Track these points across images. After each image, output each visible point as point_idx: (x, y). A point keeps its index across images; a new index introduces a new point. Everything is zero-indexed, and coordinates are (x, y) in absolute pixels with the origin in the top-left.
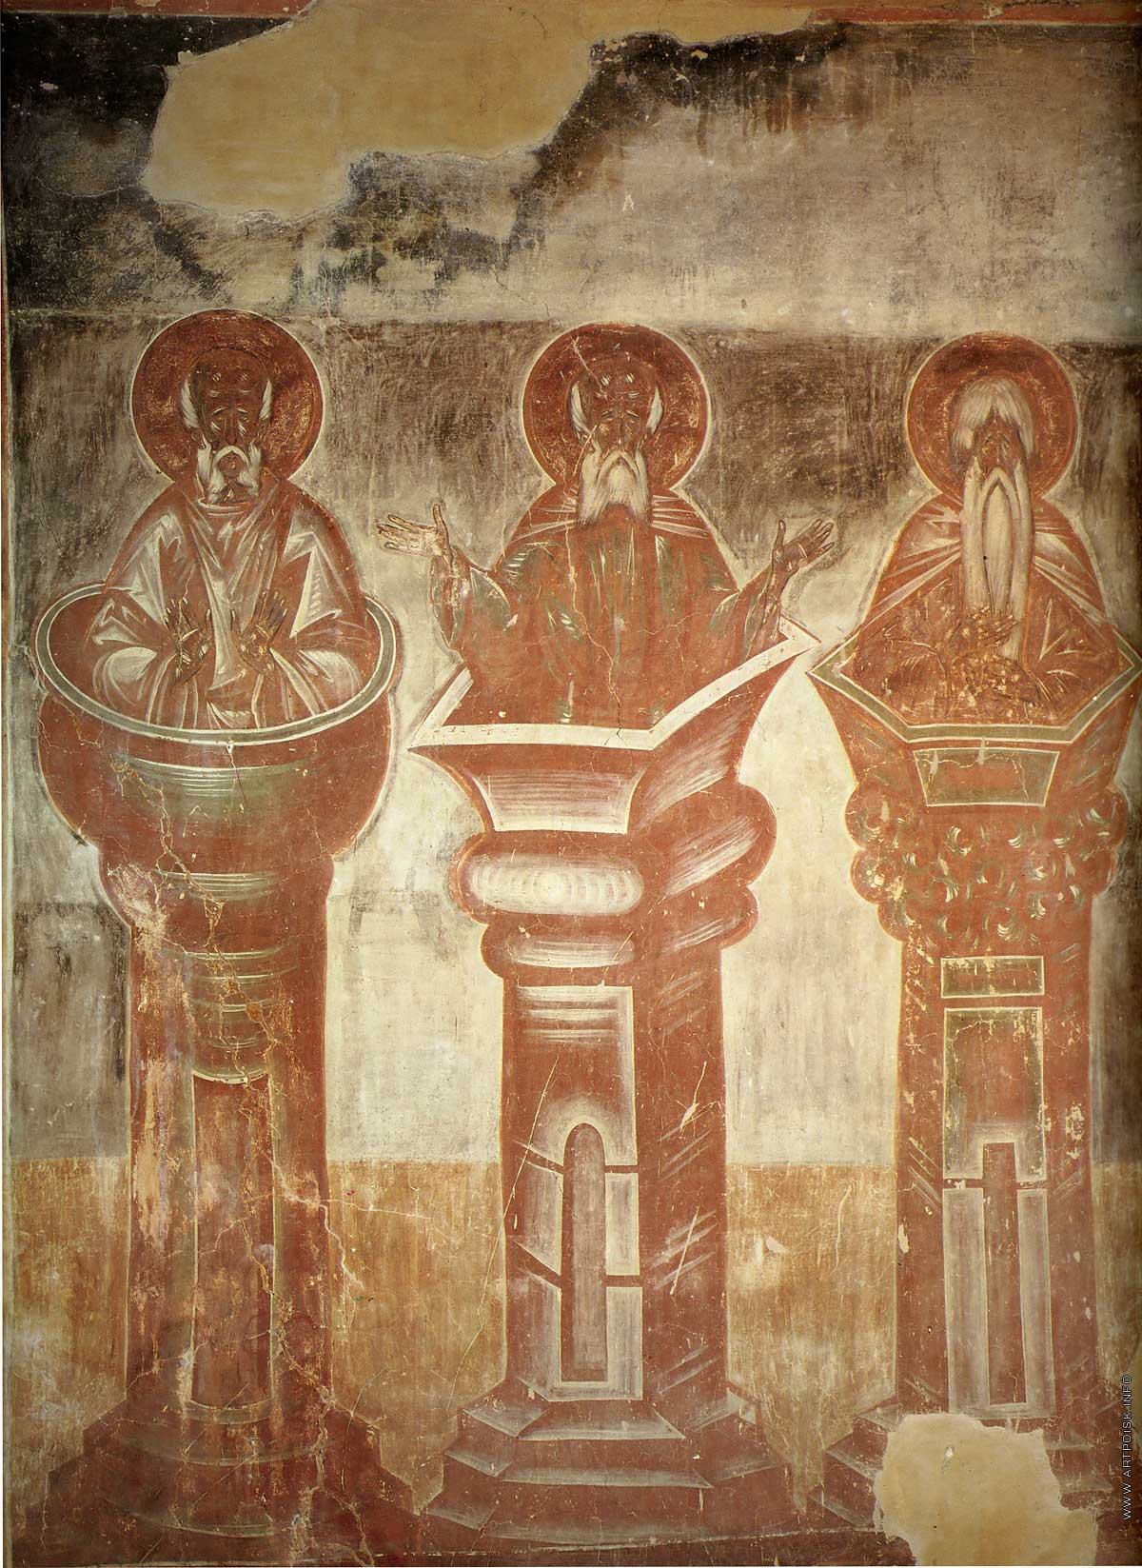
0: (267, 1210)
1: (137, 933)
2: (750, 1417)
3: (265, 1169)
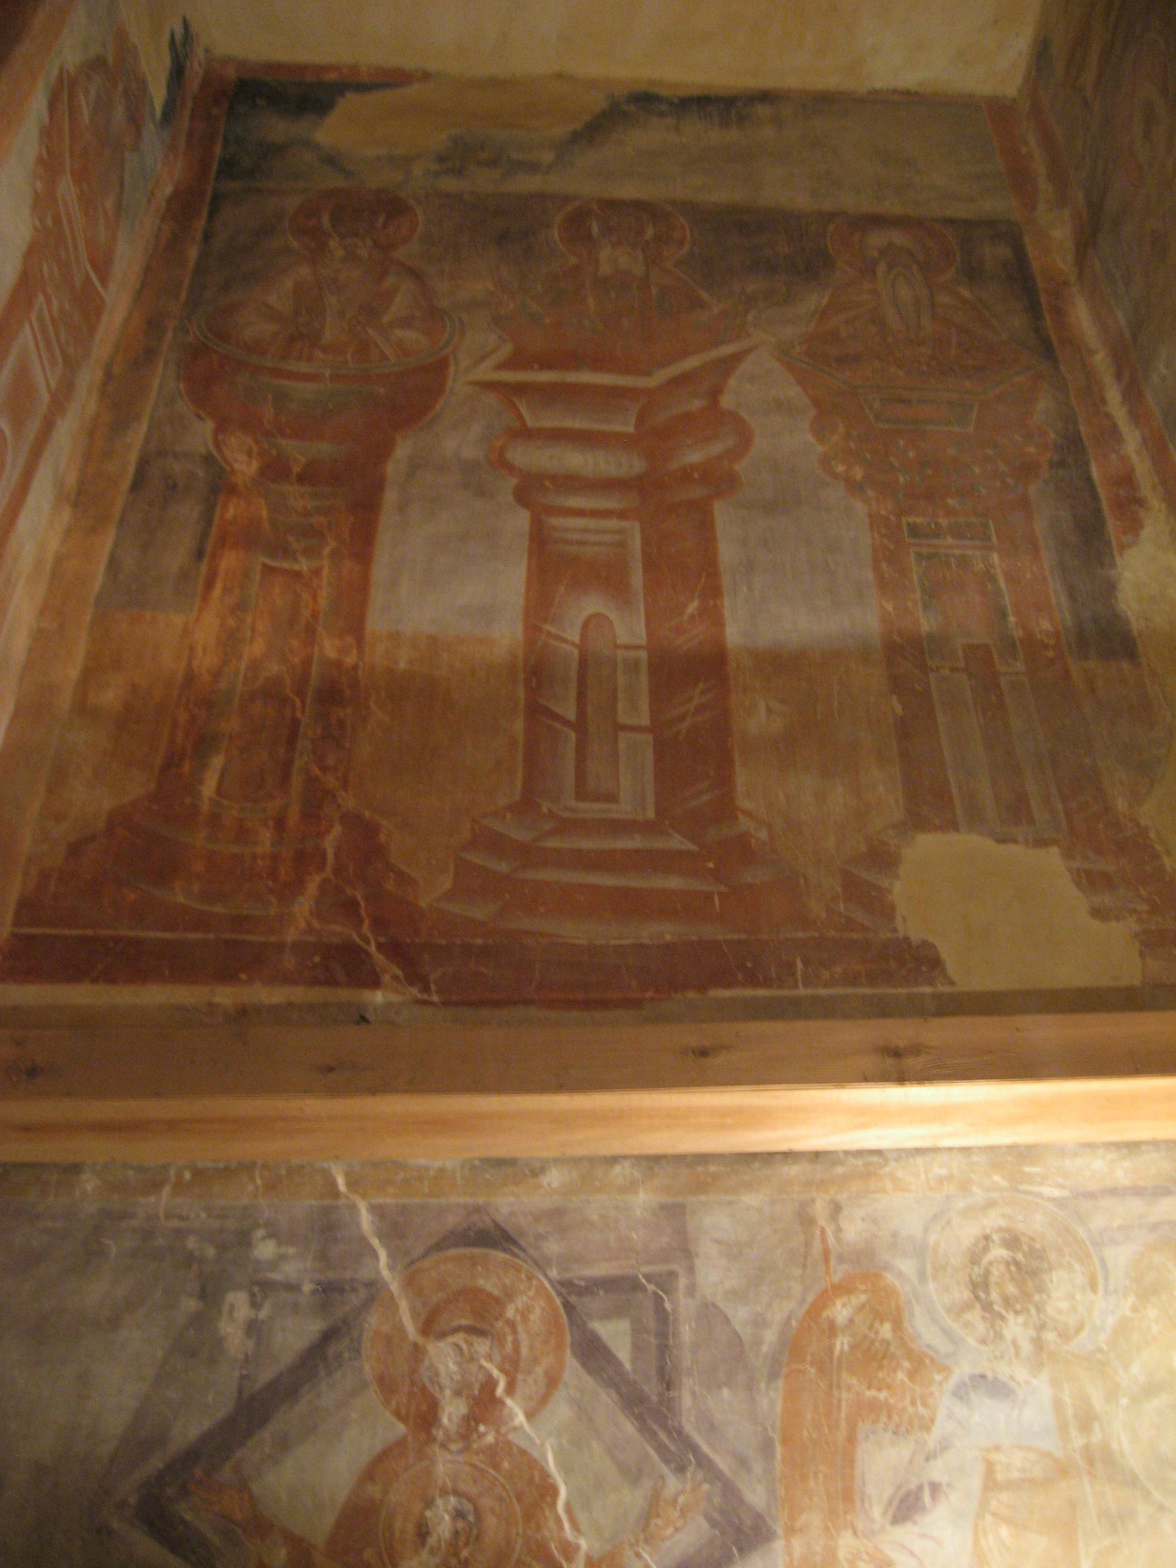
1: (233, 472)
2: (763, 835)
3: (310, 633)
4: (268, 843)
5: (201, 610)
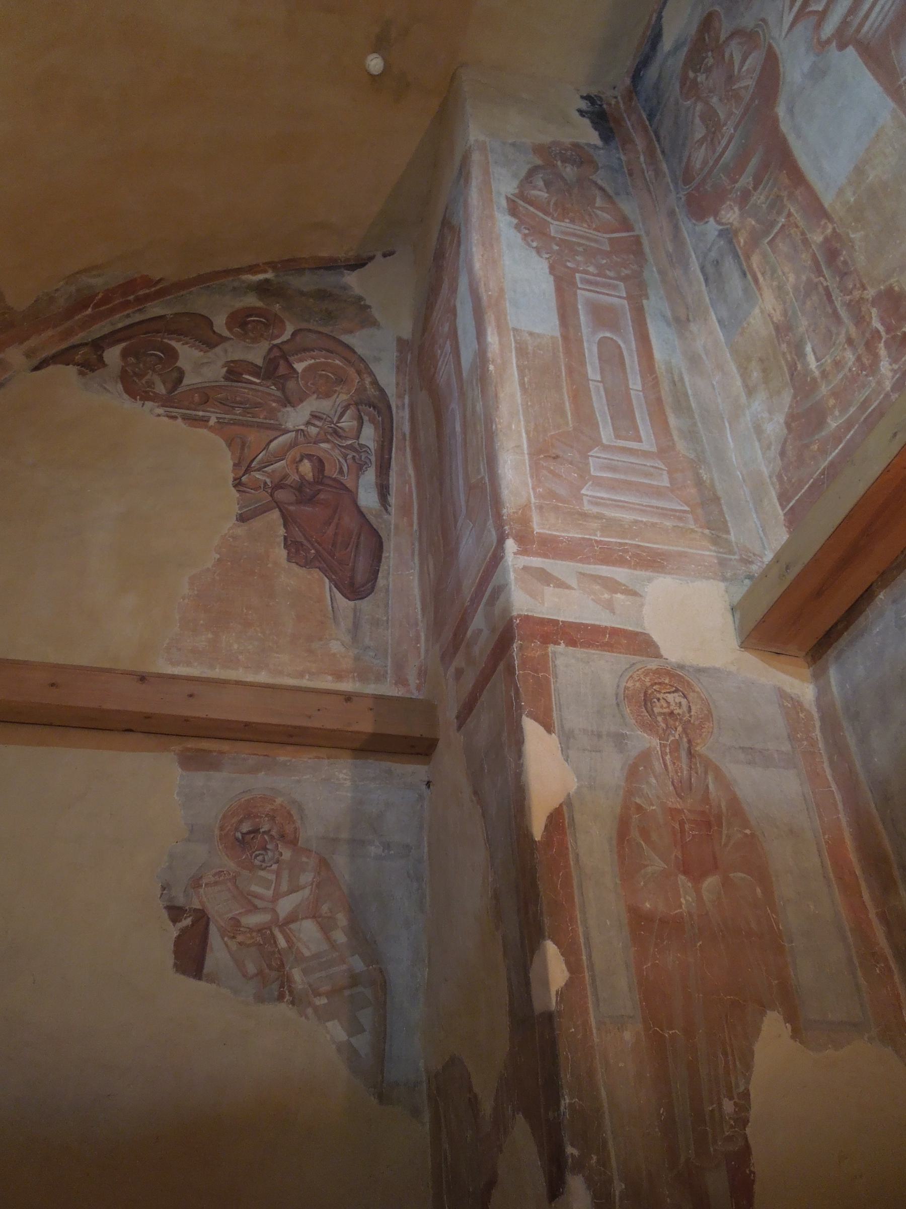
0: (814, 255)
3: (806, 242)
4: (851, 356)
5: (761, 295)
